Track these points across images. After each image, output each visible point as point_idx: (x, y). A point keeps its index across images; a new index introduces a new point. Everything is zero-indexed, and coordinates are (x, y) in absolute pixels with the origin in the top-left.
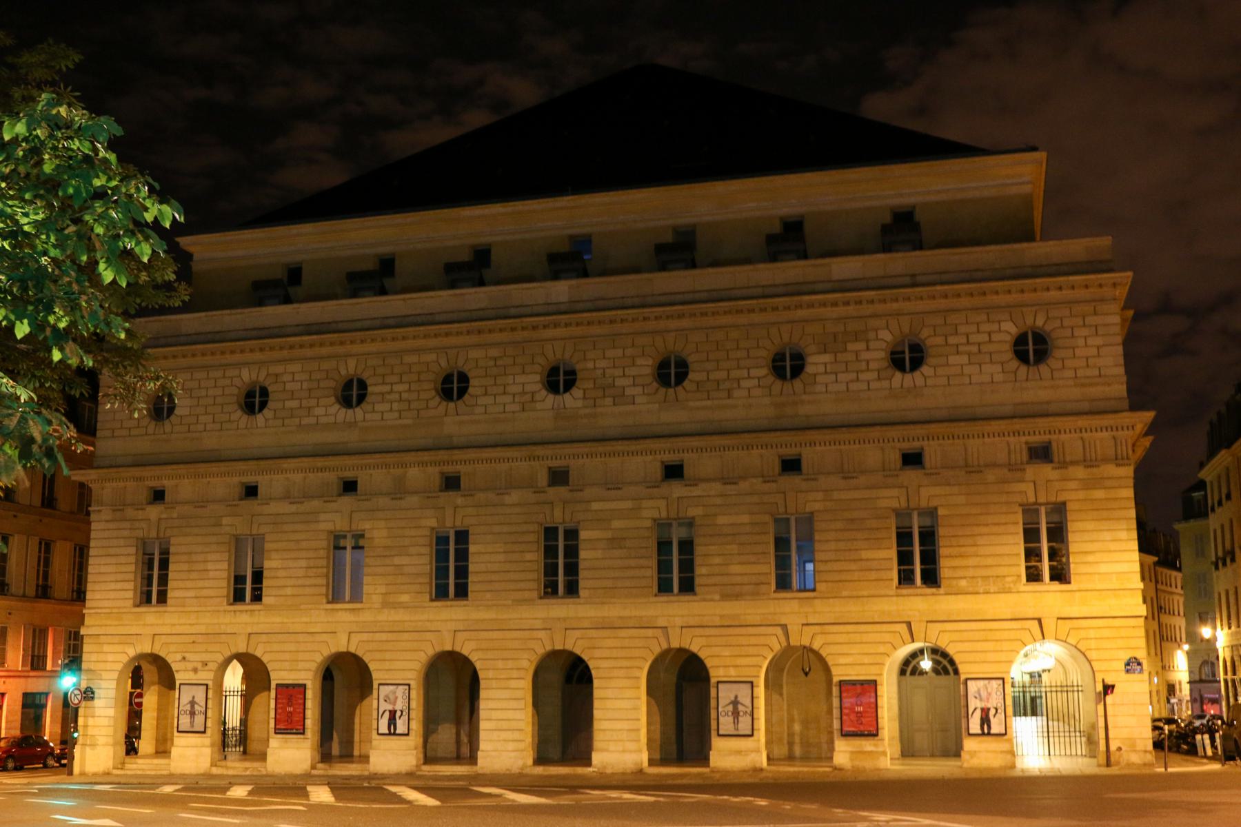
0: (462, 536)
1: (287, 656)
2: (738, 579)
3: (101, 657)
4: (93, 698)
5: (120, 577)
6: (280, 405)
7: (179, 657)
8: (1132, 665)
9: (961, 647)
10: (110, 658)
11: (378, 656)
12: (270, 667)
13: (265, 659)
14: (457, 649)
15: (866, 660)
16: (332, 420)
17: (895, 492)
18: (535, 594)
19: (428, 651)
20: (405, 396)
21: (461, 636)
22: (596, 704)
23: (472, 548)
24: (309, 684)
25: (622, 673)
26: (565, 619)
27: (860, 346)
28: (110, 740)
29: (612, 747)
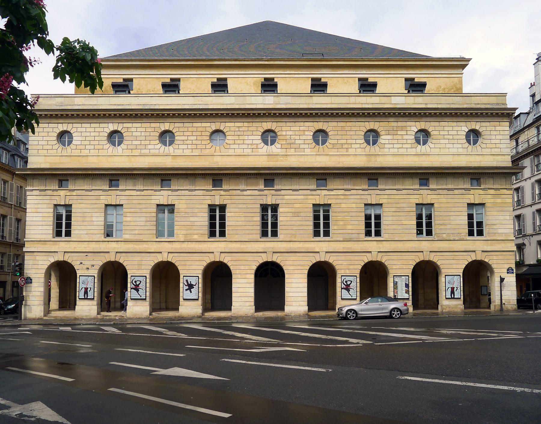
0: (223, 208)
2: (350, 232)
3: (36, 262)
4: (31, 282)
5: (44, 223)
6: (130, 143)
7: (78, 263)
8: (510, 271)
9: (443, 262)
11: (182, 263)
12: (127, 268)
13: (125, 264)
16: (156, 152)
17: (417, 196)
18: (259, 236)
20: (194, 142)
21: (223, 255)
22: (286, 285)
23: (228, 214)
25: (299, 271)
26: (273, 248)
27: (404, 133)
29: (294, 304)
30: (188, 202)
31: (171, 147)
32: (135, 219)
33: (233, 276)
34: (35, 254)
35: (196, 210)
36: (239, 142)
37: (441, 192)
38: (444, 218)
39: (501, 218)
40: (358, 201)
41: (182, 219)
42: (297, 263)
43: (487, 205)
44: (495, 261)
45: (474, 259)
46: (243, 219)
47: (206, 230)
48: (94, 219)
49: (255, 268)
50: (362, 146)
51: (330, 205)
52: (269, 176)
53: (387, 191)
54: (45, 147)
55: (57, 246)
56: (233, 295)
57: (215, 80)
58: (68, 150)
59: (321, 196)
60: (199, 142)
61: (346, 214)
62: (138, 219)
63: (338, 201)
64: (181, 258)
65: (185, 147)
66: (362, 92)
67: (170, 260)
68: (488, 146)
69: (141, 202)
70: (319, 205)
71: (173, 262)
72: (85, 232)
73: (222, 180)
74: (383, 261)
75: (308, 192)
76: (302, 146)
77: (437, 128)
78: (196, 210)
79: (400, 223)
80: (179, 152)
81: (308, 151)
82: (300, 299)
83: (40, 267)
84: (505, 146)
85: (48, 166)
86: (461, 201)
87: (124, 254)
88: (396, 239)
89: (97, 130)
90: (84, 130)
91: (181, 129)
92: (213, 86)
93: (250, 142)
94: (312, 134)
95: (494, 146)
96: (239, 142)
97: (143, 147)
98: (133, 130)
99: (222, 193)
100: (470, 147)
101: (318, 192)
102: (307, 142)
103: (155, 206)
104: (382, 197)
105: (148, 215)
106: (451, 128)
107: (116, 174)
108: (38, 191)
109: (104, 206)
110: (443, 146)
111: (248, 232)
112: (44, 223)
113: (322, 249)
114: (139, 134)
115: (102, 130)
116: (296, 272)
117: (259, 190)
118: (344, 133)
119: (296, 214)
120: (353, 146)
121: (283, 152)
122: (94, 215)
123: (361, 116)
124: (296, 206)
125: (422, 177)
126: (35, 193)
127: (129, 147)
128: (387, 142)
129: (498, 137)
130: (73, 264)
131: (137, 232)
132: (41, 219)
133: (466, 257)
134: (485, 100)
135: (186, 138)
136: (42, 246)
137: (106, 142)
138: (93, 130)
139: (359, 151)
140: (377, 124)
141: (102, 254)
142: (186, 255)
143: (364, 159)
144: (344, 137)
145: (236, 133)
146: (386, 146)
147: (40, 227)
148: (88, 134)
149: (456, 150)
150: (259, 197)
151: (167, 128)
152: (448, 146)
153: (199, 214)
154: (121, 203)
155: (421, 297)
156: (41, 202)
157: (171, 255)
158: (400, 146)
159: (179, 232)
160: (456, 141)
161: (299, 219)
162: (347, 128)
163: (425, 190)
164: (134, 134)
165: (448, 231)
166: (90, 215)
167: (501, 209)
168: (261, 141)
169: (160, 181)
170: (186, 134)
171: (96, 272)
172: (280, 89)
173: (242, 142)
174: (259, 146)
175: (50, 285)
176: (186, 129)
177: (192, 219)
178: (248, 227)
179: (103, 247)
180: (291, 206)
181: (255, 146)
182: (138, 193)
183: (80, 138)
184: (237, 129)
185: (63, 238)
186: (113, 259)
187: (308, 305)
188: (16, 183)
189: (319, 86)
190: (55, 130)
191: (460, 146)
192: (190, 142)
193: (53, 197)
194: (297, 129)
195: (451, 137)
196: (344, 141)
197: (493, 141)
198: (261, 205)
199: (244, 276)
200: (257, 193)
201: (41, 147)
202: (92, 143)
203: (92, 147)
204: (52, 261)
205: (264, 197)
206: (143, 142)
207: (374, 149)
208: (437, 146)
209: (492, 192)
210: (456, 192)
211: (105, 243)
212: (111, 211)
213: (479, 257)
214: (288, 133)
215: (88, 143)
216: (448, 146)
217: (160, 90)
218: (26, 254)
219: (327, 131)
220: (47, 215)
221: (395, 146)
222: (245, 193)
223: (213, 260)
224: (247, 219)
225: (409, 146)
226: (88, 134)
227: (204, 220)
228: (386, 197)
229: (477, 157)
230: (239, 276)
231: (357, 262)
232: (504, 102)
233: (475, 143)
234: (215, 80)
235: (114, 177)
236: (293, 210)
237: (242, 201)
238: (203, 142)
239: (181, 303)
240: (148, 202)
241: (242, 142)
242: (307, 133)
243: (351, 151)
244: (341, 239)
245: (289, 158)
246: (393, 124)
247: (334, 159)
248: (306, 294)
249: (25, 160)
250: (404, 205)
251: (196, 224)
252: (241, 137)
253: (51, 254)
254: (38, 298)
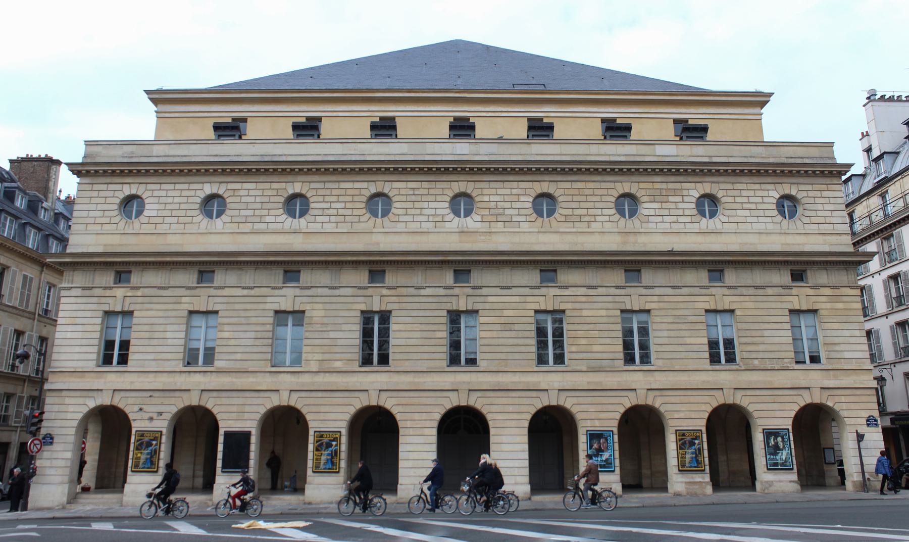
0: (385, 317)
1: (234, 409)
2: (599, 356)
3: (63, 408)
4: (51, 443)
6: (236, 213)
7: (136, 408)
8: (871, 422)
10: (71, 409)
11: (314, 409)
12: (219, 417)
14: (381, 404)
15: (693, 415)
16: (279, 226)
18: (444, 363)
19: (359, 403)
20: (341, 212)
21: (384, 395)
23: (393, 327)
24: (254, 432)
25: (513, 423)
27: (679, 199)
28: (66, 479)
30: (328, 306)
31: (302, 220)
32: (236, 335)
33: (401, 432)
34: (64, 393)
35: (340, 321)
36: (413, 212)
37: (744, 291)
38: (754, 333)
39: (847, 333)
40: (610, 306)
41: (316, 335)
42: (511, 409)
43: (822, 312)
44: (844, 406)
45: (809, 401)
46: (418, 335)
47: (356, 353)
48: (168, 335)
49: (438, 417)
50: (612, 219)
51: (563, 311)
52: (462, 266)
53: (656, 289)
54: (98, 220)
55: (103, 380)
56: (401, 464)
57: (377, 120)
58: (136, 225)
59: (549, 297)
60: (349, 212)
61: (591, 327)
62: (242, 335)
63: (577, 306)
64: (309, 401)
65: (326, 219)
66: (608, 138)
67: (292, 403)
68: (814, 220)
69: (249, 306)
70: (545, 312)
71: (298, 406)
72: (152, 357)
73: (384, 271)
74: (657, 405)
75: (527, 291)
76: (515, 219)
77: (730, 193)
78: (340, 321)
79: (681, 341)
80: (315, 227)
81: (525, 227)
82: (516, 472)
83: (69, 416)
84: (839, 220)
85: (100, 250)
86: (779, 305)
87: (215, 394)
88: (677, 368)
89: (185, 193)
90: (163, 193)
91: (321, 192)
92: (374, 127)
93: (432, 212)
94: (531, 199)
95: (822, 220)
96: (413, 212)
97: (258, 219)
98: (244, 194)
99: (385, 292)
100: (785, 222)
101: (543, 291)
102: (522, 212)
103: (272, 314)
104: (649, 298)
105: (259, 328)
106: (751, 193)
107: (210, 263)
108: (80, 290)
109: (186, 313)
110: (742, 219)
111: (426, 356)
112: (84, 342)
113: (553, 385)
114: (252, 199)
115: (192, 193)
116: (509, 424)
117: (446, 288)
118: (583, 198)
119: (507, 326)
120: (598, 219)
121: (484, 227)
122: (169, 328)
123: (608, 174)
124: (506, 313)
125: (712, 267)
126: (74, 292)
127: (235, 219)
128: (652, 212)
129: (826, 207)
130: (127, 410)
131: (239, 356)
132: (79, 335)
133: (795, 399)
134: (800, 151)
135: (327, 205)
136: (78, 380)
137: (198, 212)
138: (178, 193)
139: (608, 227)
140: (635, 186)
141: (177, 394)
142: (320, 394)
143: (618, 238)
144: (583, 205)
145: (409, 198)
146: (651, 219)
147: (77, 349)
148: (170, 200)
149: (762, 226)
150: (445, 299)
151: (297, 190)
152: (749, 219)
153: (344, 327)
154: (215, 309)
155: (723, 467)
156: (82, 307)
157: (295, 396)
158: (674, 219)
159: (310, 356)
160: (761, 213)
161: (513, 334)
162: (587, 192)
163: (719, 289)
164: (244, 199)
165: (761, 355)
166: (162, 328)
167: (844, 319)
168: (448, 211)
169: (282, 272)
170: (327, 199)
171: (166, 424)
172: (479, 133)
173: (418, 212)
174: (447, 218)
175: (83, 449)
176: (328, 192)
177: (332, 335)
178: (426, 349)
179: (181, 381)
180: (498, 313)
181: (439, 219)
182: (245, 292)
183: (156, 207)
184: (411, 192)
185: (115, 367)
186: (195, 402)
187: (531, 482)
188: (48, 277)
189: (540, 129)
190: (117, 194)
191: (769, 220)
192: (335, 212)
193: (103, 300)
194: (508, 191)
195: (753, 206)
196: (584, 212)
197: (820, 213)
198: (449, 311)
199: (419, 432)
200: (442, 292)
201: (92, 221)
202: (175, 213)
203: (175, 220)
204: (92, 404)
205: (454, 299)
206: (257, 212)
207: (634, 224)
208: (732, 219)
209: (828, 291)
210: (770, 291)
211: (184, 375)
212: (198, 321)
213: (817, 398)
214: (493, 198)
215: (168, 213)
216: (749, 219)
217: (290, 133)
218: (48, 394)
219: (556, 195)
220: (90, 328)
221: (666, 219)
222: (423, 292)
223: (366, 404)
224: (425, 334)
225: (688, 219)
226: (170, 200)
227: (352, 335)
228: (656, 298)
229: (797, 237)
230: (411, 431)
231: (611, 408)
232: (830, 156)
233: (792, 215)
234: (377, 120)
235: (206, 267)
236: (503, 320)
237: (418, 306)
238: (356, 212)
239: (308, 479)
240: (261, 306)
241: (418, 212)
242: (522, 198)
243: (595, 227)
244: (584, 369)
245: (495, 238)
246: (659, 184)
247: (569, 238)
248: (526, 463)
249: (63, 241)
250: (686, 312)
251: (340, 342)
252: (417, 205)
253: (91, 394)
254: (60, 471)
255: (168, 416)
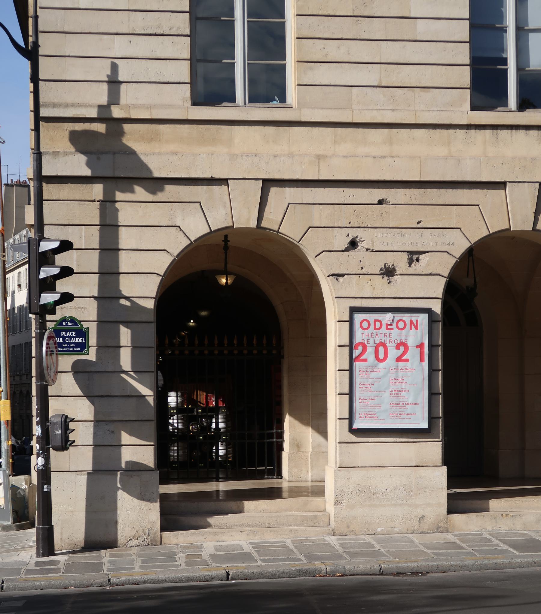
7: (341, 240)
72: (370, 76)
204: (196, 228)
255: (445, 265)
